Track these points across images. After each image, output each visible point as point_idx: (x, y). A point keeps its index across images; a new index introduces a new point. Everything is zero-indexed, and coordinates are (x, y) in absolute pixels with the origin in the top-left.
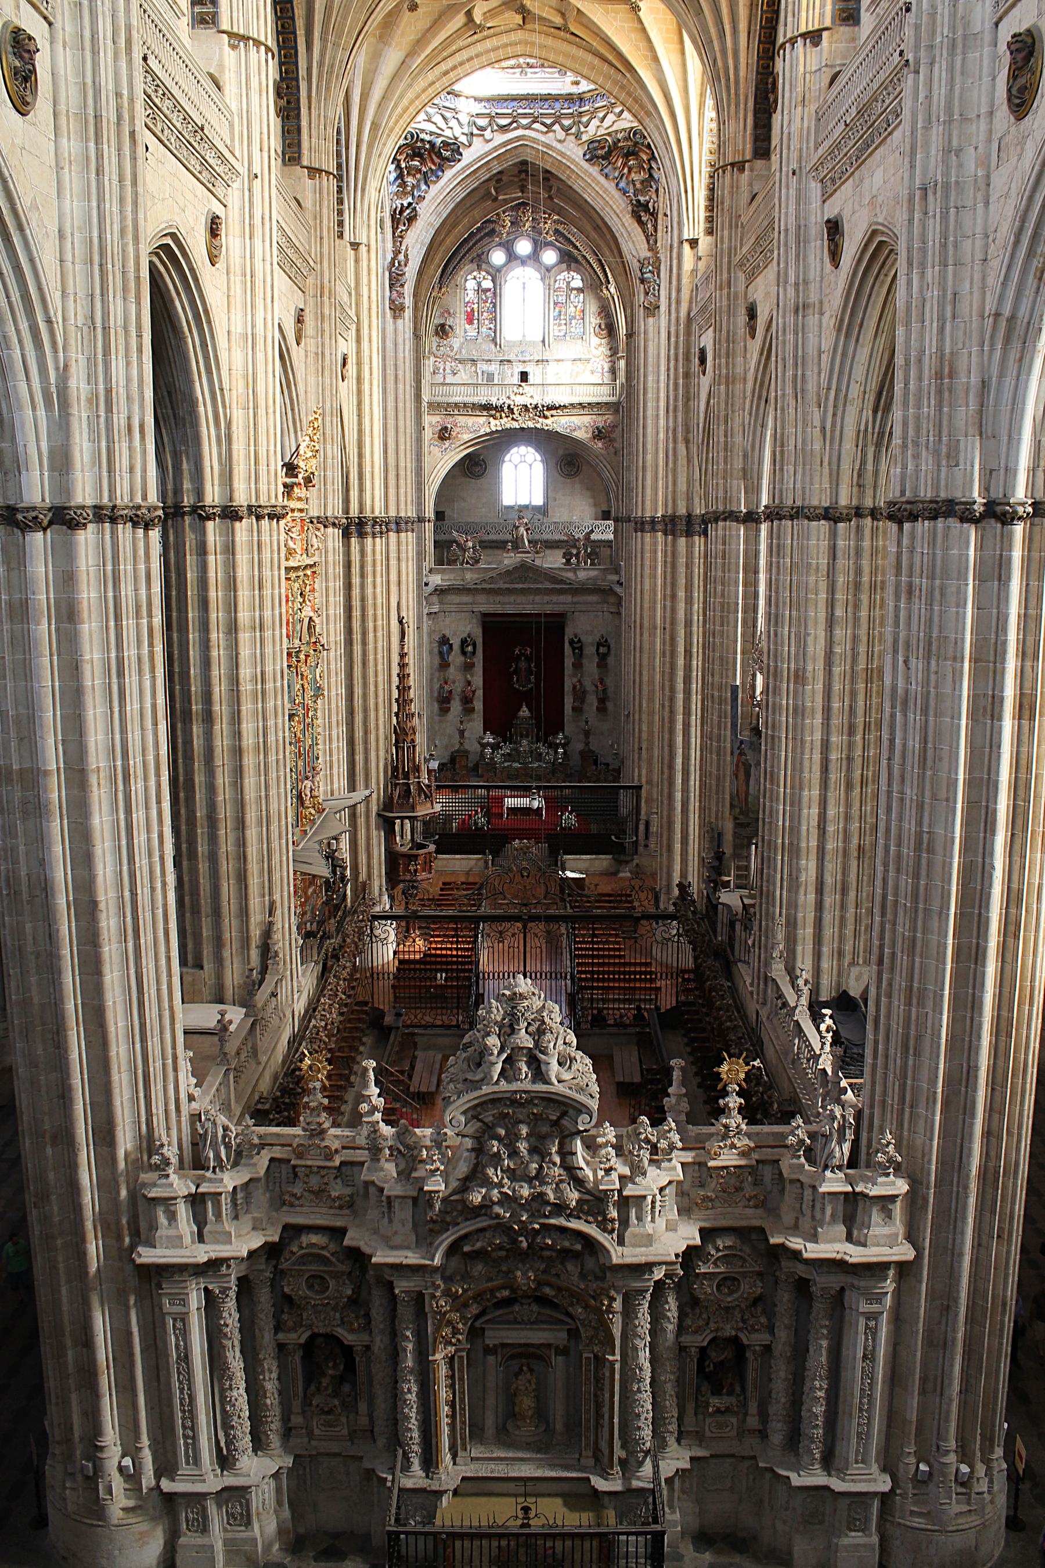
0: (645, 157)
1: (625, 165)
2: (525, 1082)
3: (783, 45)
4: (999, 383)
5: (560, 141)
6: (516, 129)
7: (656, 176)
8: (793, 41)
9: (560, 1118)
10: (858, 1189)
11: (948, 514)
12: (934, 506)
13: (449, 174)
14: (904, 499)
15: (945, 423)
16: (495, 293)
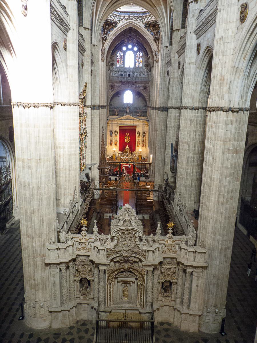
0: (157, 27)
1: (153, 29)
2: (127, 226)
3: (189, 3)
4: (234, 82)
5: (139, 23)
6: (129, 19)
7: (159, 31)
8: (192, 2)
9: (135, 234)
10: (196, 251)
11: (221, 110)
12: (218, 108)
13: (115, 29)
14: (212, 107)
15: (221, 90)
16: (123, 57)
